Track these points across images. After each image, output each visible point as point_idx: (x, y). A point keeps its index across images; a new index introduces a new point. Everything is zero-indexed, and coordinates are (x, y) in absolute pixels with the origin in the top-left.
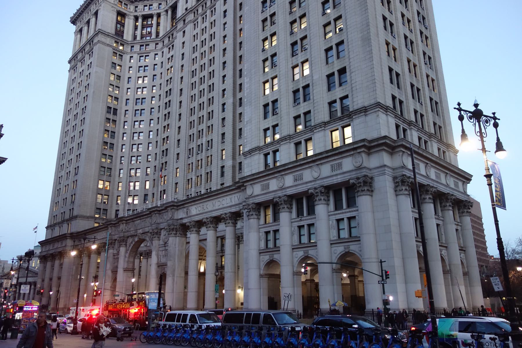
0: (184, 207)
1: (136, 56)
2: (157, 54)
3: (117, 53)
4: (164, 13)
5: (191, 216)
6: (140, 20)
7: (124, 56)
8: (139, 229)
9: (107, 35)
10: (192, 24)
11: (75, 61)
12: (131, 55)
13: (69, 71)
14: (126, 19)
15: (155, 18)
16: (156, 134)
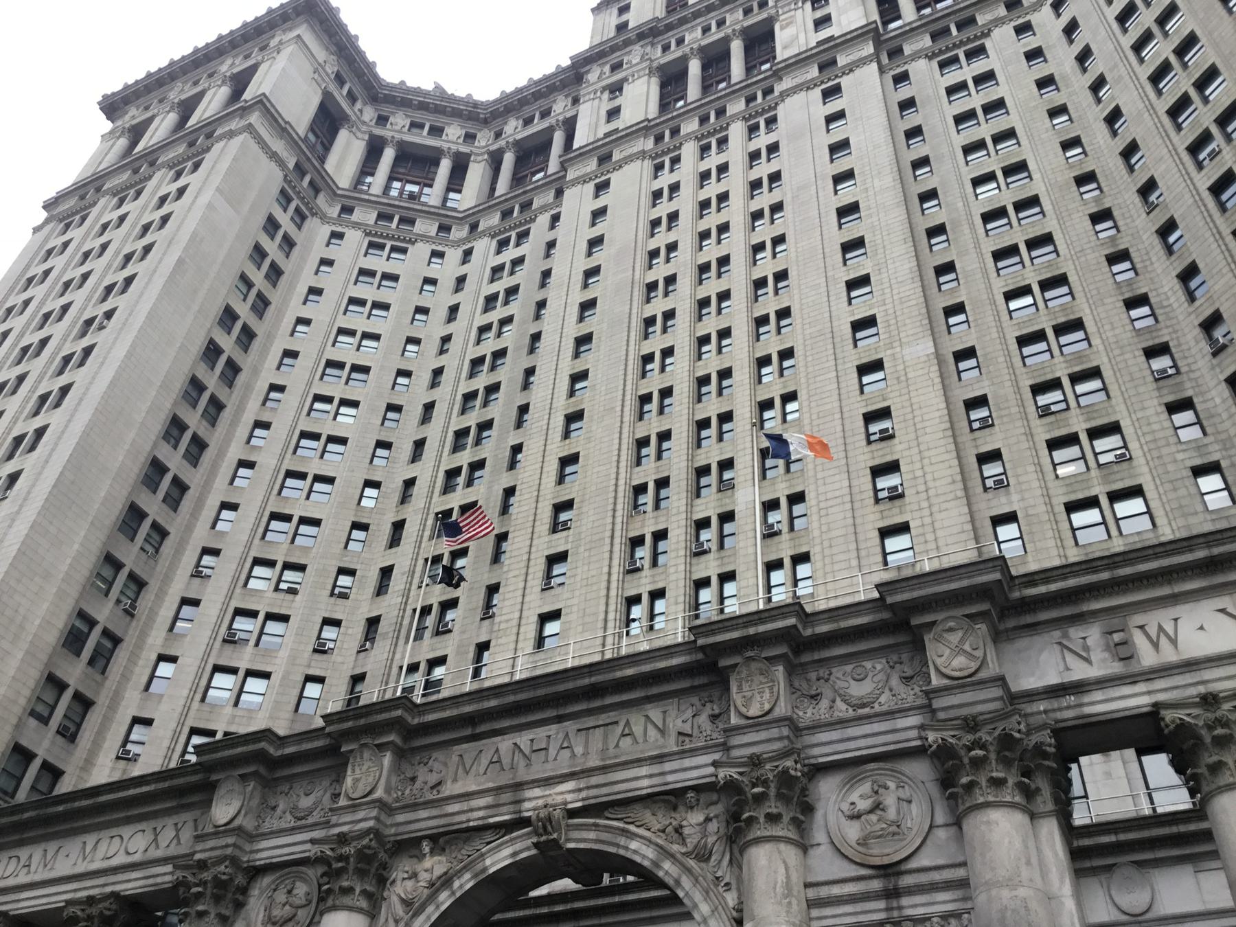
0: (1079, 619)
1: (354, 239)
2: (441, 255)
3: (289, 200)
4: (486, 157)
5: (1191, 665)
6: (389, 155)
7: (312, 223)
8: (547, 782)
9: (282, 129)
10: (648, 165)
11: (68, 208)
12: (339, 229)
13: (36, 230)
14: (343, 135)
15: (445, 166)
16: (396, 497)
